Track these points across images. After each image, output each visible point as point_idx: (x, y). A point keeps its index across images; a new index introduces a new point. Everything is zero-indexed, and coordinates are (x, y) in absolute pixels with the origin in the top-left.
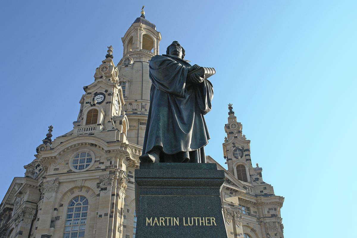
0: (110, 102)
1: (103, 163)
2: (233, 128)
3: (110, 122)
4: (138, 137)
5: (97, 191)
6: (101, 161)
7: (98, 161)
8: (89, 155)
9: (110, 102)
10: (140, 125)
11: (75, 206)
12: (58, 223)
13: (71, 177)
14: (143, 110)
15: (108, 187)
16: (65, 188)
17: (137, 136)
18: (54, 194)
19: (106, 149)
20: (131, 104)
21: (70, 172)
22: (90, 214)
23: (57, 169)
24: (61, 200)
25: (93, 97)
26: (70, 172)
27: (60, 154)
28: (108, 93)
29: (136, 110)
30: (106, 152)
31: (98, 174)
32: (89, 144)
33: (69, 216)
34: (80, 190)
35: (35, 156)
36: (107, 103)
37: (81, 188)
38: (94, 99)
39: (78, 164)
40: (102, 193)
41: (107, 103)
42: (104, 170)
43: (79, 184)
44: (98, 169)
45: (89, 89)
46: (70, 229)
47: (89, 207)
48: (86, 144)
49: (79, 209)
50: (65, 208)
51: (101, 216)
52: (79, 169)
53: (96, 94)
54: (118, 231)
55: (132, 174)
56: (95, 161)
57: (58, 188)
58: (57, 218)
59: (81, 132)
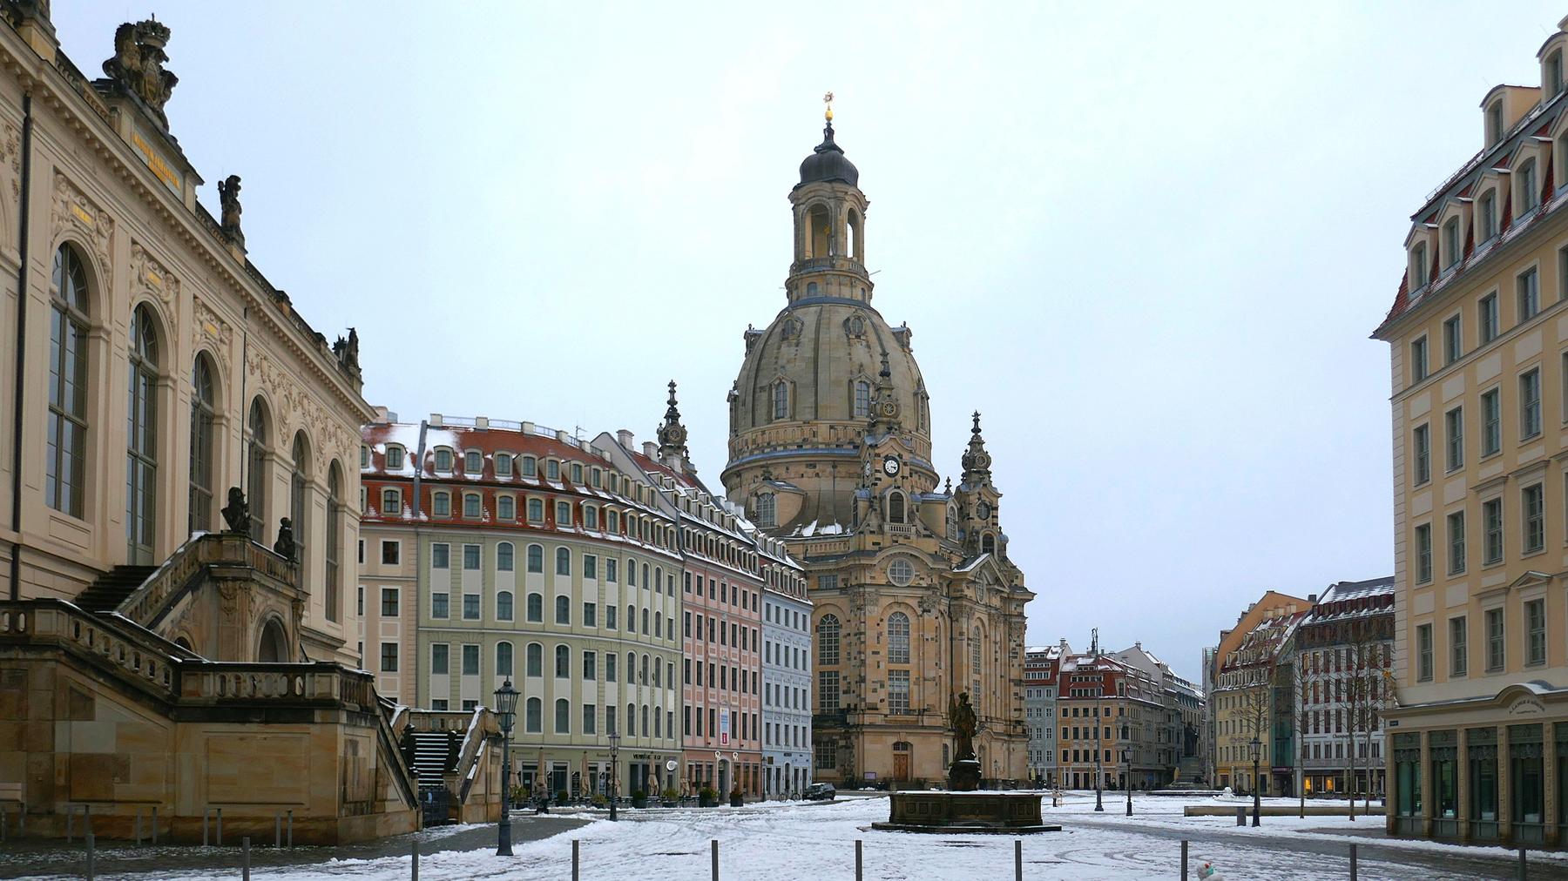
2: (976, 462)
13: (893, 591)
21: (889, 585)
22: (913, 635)
31: (920, 593)
33: (890, 633)
44: (919, 587)
50: (886, 624)
53: (887, 458)
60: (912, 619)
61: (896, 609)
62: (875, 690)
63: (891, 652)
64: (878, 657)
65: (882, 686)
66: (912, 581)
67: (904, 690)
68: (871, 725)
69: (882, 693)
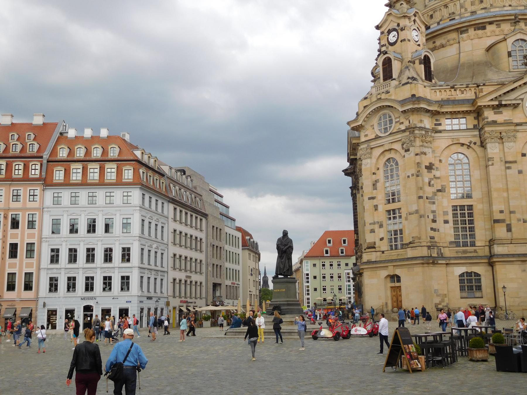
0: (404, 40)
1: (402, 123)
3: (407, 67)
4: (460, 53)
5: (402, 152)
6: (401, 121)
7: (398, 121)
8: (390, 117)
9: (404, 40)
10: (461, 34)
11: (389, 168)
12: (378, 185)
13: (379, 142)
14: (463, 10)
15: (411, 149)
16: (377, 152)
17: (458, 52)
18: (369, 161)
19: (401, 109)
20: (447, 7)
21: (377, 137)
23: (366, 136)
24: (376, 164)
25: (387, 36)
26: (377, 137)
27: (364, 121)
28: (400, 27)
29: (453, 13)
30: (402, 112)
31: (399, 136)
32: (386, 106)
33: (387, 177)
34: (389, 152)
35: (372, 81)
36: (401, 41)
37: (391, 149)
38: (388, 38)
39: (383, 127)
40: (406, 154)
41: (401, 41)
42: (404, 131)
43: (387, 147)
45: (381, 27)
46: (388, 189)
47: (399, 168)
48: (383, 106)
49: (392, 170)
50: (381, 171)
51: (409, 177)
52: (385, 133)
53: (389, 32)
54: (429, 186)
55: (439, 121)
56: (396, 122)
57: (371, 153)
58: (377, 181)
59: (379, 92)
60: (400, 163)
61: (388, 155)
62: (372, 231)
63: (387, 195)
64: (375, 202)
65: (381, 226)
66: (395, 127)
67: (401, 227)
68: (369, 262)
69: (381, 233)
